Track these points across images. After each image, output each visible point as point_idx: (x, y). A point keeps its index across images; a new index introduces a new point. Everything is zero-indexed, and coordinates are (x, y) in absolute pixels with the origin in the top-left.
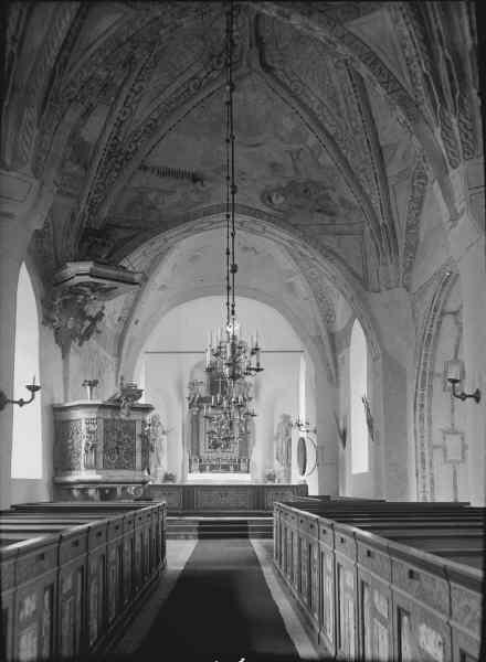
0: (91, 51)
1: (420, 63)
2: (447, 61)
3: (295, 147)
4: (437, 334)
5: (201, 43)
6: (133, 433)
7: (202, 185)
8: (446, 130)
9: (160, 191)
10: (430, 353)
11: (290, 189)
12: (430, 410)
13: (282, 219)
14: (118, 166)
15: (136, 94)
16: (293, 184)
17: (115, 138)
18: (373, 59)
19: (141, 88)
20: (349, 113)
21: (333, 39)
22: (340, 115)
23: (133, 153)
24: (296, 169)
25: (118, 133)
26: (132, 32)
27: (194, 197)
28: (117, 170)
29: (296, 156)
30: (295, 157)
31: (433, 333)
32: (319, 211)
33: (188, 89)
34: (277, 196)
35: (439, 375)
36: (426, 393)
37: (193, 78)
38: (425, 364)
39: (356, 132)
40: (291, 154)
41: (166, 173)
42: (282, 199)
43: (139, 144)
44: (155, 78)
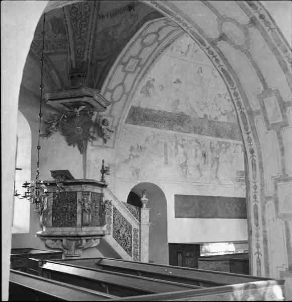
4: (229, 65)
6: (74, 201)
10: (237, 90)
12: (260, 156)
27: (131, 21)
31: (225, 67)
35: (258, 113)
36: (251, 135)
38: (239, 103)
41: (115, 14)
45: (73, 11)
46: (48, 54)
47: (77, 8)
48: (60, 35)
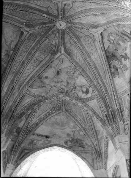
0: (23, 107)
1: (104, 112)
2: (111, 112)
3: (74, 130)
7: (49, 139)
8: (112, 128)
9: (39, 140)
11: (72, 141)
13: (69, 148)
14: (27, 133)
15: (33, 116)
16: (73, 139)
18: (93, 110)
19: (35, 115)
20: (87, 122)
21: (83, 106)
22: (85, 122)
23: (32, 130)
24: (74, 136)
25: (28, 125)
26: (34, 103)
27: (47, 142)
28: (27, 134)
29: (74, 132)
30: (74, 132)
32: (80, 147)
33: (47, 115)
34: (69, 142)
37: (48, 113)
39: (89, 127)
40: (73, 132)
41: (40, 135)
42: (70, 143)
43: (33, 128)
44: (38, 112)
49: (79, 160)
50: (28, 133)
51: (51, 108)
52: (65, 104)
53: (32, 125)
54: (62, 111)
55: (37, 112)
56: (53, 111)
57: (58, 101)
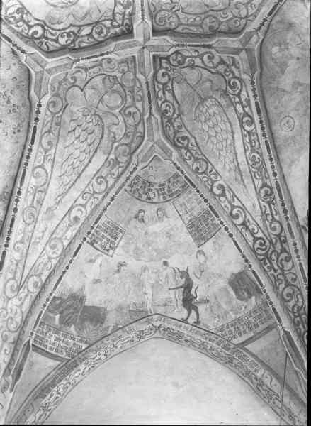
5: (208, 103)
14: (284, 255)
15: (224, 195)
17: (256, 239)
19: (221, 186)
25: (252, 234)
33: (249, 133)
37: (241, 121)
44: (219, 167)
45: (257, 246)
46: (243, 343)
47: (260, 238)
48: (253, 298)
49: (305, 66)
50: (284, 250)
51: (224, 102)
52: (211, 28)
53: (264, 215)
54: (243, 54)
55: (217, 173)
56: (239, 95)
57: (198, 62)
